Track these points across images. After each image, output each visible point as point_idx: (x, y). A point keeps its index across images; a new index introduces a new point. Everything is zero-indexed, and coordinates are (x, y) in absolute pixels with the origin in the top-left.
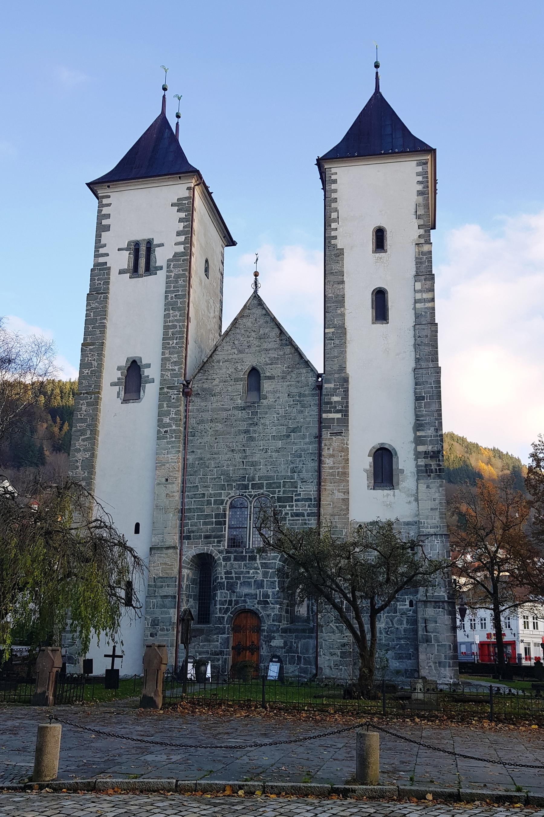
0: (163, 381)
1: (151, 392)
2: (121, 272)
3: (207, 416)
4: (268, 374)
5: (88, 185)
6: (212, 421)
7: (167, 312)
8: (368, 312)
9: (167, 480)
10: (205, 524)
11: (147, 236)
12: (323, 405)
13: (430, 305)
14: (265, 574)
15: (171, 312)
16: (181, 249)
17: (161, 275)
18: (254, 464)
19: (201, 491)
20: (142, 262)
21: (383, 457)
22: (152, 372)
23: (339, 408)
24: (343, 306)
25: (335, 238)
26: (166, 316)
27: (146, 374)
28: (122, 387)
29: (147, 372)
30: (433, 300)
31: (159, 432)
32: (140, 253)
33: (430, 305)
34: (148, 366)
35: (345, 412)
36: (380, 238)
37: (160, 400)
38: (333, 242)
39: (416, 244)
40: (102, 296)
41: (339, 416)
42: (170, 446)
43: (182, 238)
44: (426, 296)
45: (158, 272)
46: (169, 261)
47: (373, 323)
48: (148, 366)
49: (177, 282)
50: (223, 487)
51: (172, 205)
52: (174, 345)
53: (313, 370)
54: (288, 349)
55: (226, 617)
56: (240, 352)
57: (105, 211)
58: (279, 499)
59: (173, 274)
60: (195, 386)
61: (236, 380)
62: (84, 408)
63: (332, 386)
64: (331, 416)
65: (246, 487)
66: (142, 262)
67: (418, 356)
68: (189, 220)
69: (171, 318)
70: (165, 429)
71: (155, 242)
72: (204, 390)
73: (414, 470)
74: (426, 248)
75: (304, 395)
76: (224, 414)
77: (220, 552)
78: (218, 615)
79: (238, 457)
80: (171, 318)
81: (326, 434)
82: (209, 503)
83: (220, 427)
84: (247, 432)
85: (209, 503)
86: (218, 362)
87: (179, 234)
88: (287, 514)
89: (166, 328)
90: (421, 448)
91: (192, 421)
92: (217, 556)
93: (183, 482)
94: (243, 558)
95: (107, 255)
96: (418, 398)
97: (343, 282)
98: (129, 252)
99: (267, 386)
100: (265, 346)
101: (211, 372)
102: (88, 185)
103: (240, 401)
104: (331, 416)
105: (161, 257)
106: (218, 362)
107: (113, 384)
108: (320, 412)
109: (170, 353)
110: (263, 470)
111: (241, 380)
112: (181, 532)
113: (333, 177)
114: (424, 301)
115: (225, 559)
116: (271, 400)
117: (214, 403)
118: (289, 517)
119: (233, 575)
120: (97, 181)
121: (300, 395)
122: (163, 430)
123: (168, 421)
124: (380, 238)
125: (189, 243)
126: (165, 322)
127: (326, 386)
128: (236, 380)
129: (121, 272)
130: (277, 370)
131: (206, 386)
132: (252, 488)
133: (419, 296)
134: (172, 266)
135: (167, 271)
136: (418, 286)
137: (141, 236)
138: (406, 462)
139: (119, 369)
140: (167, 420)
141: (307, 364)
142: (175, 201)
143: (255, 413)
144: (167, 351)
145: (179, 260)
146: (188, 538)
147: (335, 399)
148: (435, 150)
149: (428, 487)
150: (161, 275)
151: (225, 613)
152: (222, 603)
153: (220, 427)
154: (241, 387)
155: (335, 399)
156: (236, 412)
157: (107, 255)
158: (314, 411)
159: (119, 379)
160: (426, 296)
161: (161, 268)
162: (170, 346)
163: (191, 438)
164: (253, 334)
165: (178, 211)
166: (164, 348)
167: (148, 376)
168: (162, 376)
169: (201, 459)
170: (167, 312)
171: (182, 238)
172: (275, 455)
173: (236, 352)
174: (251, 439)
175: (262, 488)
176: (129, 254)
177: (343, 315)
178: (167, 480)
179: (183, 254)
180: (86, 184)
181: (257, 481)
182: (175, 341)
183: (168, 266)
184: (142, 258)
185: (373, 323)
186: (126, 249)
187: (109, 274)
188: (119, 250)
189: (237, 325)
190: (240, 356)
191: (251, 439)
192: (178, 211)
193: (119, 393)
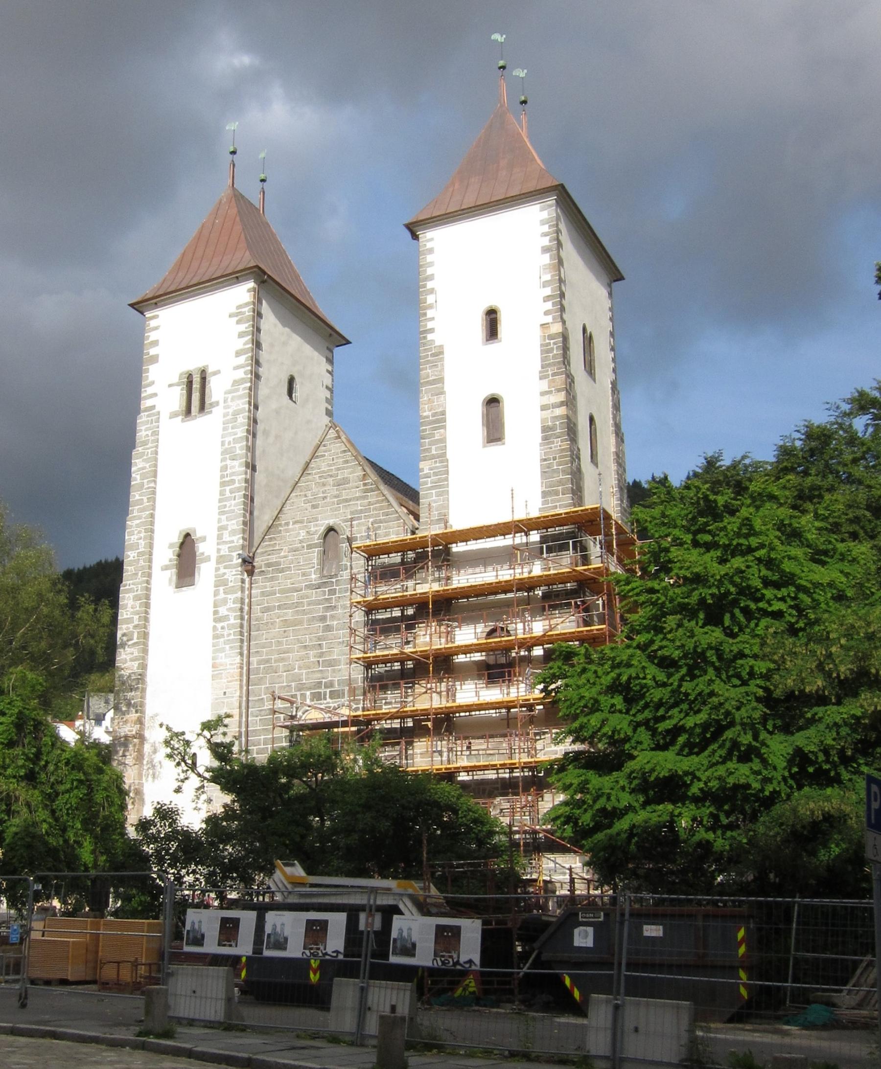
0: (221, 559)
2: (174, 415)
6: (279, 607)
7: (224, 463)
8: (478, 430)
9: (225, 693)
11: (200, 365)
15: (228, 462)
18: (331, 663)
20: (196, 396)
24: (444, 427)
25: (432, 331)
26: (224, 468)
28: (174, 571)
31: (215, 628)
32: (194, 386)
34: (204, 539)
36: (492, 322)
37: (216, 586)
38: (430, 337)
39: (542, 325)
40: (149, 451)
42: (227, 647)
45: (213, 409)
47: (484, 446)
48: (204, 539)
49: (235, 420)
51: (230, 316)
52: (232, 508)
56: (314, 507)
59: (231, 411)
60: (258, 561)
61: (310, 547)
62: (130, 603)
66: (196, 396)
69: (229, 471)
70: (222, 624)
71: (210, 370)
80: (229, 471)
83: (289, 614)
84: (323, 619)
87: (238, 354)
89: (223, 484)
95: (155, 395)
97: (443, 393)
98: (180, 387)
103: (313, 576)
105: (217, 389)
106: (287, 524)
107: (165, 568)
109: (228, 519)
111: (315, 546)
117: (284, 582)
122: (219, 625)
123: (226, 613)
124: (492, 322)
126: (222, 477)
129: (174, 415)
131: (273, 559)
132: (331, 698)
134: (229, 400)
135: (225, 408)
140: (223, 611)
142: (234, 310)
144: (224, 517)
145: (237, 390)
153: (289, 614)
157: (155, 395)
159: (170, 560)
161: (217, 403)
162: (227, 509)
164: (330, 480)
165: (238, 322)
166: (222, 513)
167: (203, 554)
168: (219, 550)
169: (268, 661)
170: (224, 463)
173: (309, 509)
174: (328, 628)
175: (343, 697)
176: (182, 390)
177: (443, 440)
178: (225, 693)
180: (132, 305)
181: (336, 687)
182: (233, 502)
183: (225, 401)
185: (484, 446)
186: (178, 385)
187: (158, 421)
188: (170, 386)
191: (328, 628)
192: (238, 322)
193: (170, 580)
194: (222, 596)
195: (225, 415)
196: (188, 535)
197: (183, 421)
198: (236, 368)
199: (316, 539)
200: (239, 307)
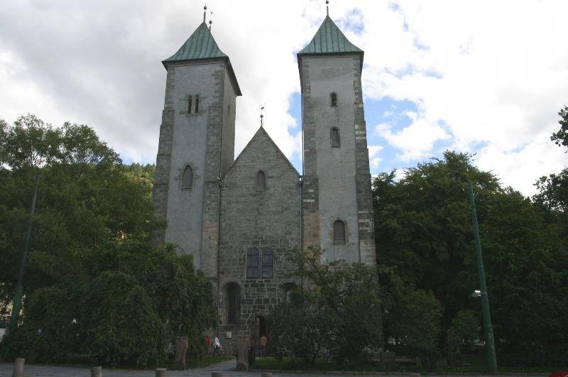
1: (199, 184)
3: (231, 199)
4: (269, 175)
5: (163, 62)
10: (233, 265)
12: (305, 194)
13: (364, 138)
14: (270, 295)
16: (218, 100)
17: (205, 116)
18: (262, 229)
19: (230, 244)
20: (193, 107)
21: (340, 225)
22: (200, 172)
23: (313, 196)
27: (197, 173)
29: (196, 172)
30: (365, 135)
33: (364, 138)
35: (317, 199)
41: (313, 201)
43: (217, 95)
44: (361, 133)
46: (210, 107)
48: (197, 168)
50: (243, 243)
53: (297, 174)
54: (281, 161)
55: (247, 320)
57: (172, 77)
58: (278, 250)
63: (309, 183)
64: (309, 201)
65: (257, 243)
66: (193, 107)
67: (358, 167)
68: (222, 83)
72: (231, 183)
73: (357, 233)
74: (360, 106)
75: (292, 188)
76: (243, 199)
77: (243, 281)
78: (243, 319)
79: (252, 224)
81: (305, 212)
82: (235, 252)
84: (257, 209)
85: (235, 252)
86: (240, 166)
87: (216, 92)
88: (282, 259)
90: (361, 221)
91: (224, 203)
92: (240, 283)
93: (220, 238)
94: (256, 285)
95: (172, 103)
96: (358, 191)
99: (269, 182)
100: (268, 158)
101: (235, 173)
102: (163, 62)
104: (309, 201)
105: (204, 104)
108: (303, 198)
110: (269, 233)
112: (218, 269)
113: (307, 64)
114: (360, 135)
115: (246, 286)
116: (271, 190)
118: (284, 261)
119: (251, 295)
120: (173, 59)
121: (290, 188)
125: (222, 96)
127: (305, 183)
128: (251, 178)
130: (275, 173)
133: (357, 133)
136: (357, 127)
137: (193, 93)
138: (352, 227)
139: (180, 170)
141: (294, 170)
143: (262, 198)
146: (223, 273)
147: (311, 191)
148: (359, 54)
149: (365, 243)
150: (205, 116)
151: (246, 318)
152: (244, 312)
154: (253, 182)
155: (311, 191)
156: (250, 197)
157: (172, 103)
158: (298, 198)
160: (361, 133)
163: (223, 213)
171: (217, 95)
172: (275, 224)
174: (260, 214)
179: (218, 103)
181: (264, 239)
184: (193, 104)
186: (184, 100)
187: (173, 114)
189: (251, 146)
190: (253, 164)
191: (260, 214)
194: (208, 194)
195: (209, 116)
196: (188, 166)
197: (186, 116)
198: (214, 97)
199: (253, 175)
200: (216, 72)
